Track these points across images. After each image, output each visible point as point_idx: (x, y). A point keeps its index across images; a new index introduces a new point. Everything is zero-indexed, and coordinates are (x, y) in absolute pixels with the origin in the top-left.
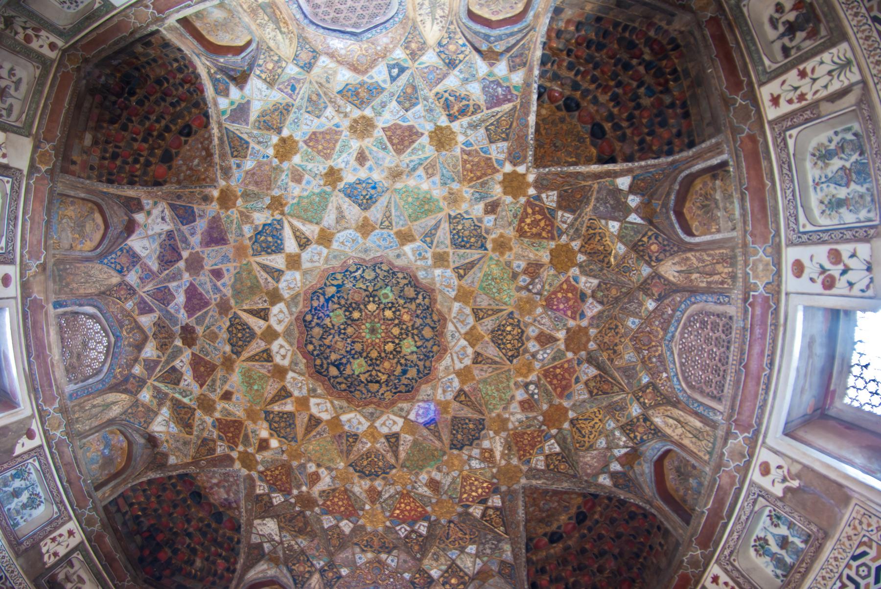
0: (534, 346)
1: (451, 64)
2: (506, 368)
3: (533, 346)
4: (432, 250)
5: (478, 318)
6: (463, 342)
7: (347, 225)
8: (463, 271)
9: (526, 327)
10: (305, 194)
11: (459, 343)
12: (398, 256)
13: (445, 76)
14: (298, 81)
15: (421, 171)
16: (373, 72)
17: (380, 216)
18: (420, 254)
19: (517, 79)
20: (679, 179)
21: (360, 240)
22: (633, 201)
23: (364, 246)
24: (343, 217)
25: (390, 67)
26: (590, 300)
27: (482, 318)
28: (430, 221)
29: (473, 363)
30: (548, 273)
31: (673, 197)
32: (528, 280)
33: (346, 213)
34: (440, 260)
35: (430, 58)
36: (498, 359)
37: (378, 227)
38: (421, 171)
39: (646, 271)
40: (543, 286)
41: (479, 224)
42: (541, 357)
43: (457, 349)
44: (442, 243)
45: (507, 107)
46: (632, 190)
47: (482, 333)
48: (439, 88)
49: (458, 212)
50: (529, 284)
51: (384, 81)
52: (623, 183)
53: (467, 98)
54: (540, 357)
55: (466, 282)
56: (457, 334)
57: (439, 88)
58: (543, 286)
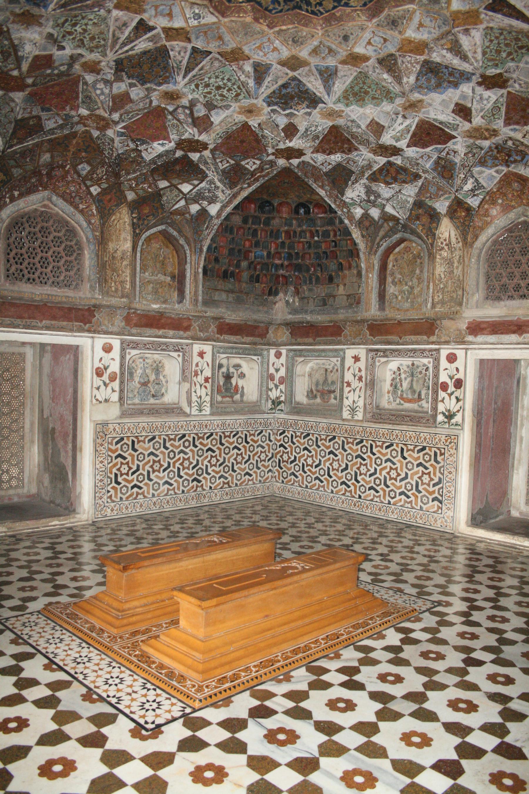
0: (119, 88)
1: (418, 204)
2: (108, 52)
3: (120, 87)
4: (312, 65)
5: (194, 50)
6: (178, 23)
7: (443, 41)
8: (261, 72)
9: (147, 89)
11: (181, 18)
12: (346, 38)
13: (418, 194)
19: (357, 211)
20: (186, 247)
22: (194, 208)
23: (400, 28)
24: (450, 50)
26: (132, 146)
27: (192, 54)
28: (339, 86)
29: (142, 19)
30: (190, 132)
31: (175, 233)
32: (196, 115)
35: (441, 206)
36: (126, 48)
37: (397, 54)
39: (131, 196)
40: (178, 120)
41: (288, 111)
42: (98, 86)
43: (176, 10)
44: (307, 75)
46: (203, 212)
47: (174, 43)
48: (420, 183)
49: (318, 109)
50: (192, 113)
52: (213, 209)
54: (100, 85)
55: (248, 68)
56: (196, 23)
57: (420, 183)
58: (178, 120)
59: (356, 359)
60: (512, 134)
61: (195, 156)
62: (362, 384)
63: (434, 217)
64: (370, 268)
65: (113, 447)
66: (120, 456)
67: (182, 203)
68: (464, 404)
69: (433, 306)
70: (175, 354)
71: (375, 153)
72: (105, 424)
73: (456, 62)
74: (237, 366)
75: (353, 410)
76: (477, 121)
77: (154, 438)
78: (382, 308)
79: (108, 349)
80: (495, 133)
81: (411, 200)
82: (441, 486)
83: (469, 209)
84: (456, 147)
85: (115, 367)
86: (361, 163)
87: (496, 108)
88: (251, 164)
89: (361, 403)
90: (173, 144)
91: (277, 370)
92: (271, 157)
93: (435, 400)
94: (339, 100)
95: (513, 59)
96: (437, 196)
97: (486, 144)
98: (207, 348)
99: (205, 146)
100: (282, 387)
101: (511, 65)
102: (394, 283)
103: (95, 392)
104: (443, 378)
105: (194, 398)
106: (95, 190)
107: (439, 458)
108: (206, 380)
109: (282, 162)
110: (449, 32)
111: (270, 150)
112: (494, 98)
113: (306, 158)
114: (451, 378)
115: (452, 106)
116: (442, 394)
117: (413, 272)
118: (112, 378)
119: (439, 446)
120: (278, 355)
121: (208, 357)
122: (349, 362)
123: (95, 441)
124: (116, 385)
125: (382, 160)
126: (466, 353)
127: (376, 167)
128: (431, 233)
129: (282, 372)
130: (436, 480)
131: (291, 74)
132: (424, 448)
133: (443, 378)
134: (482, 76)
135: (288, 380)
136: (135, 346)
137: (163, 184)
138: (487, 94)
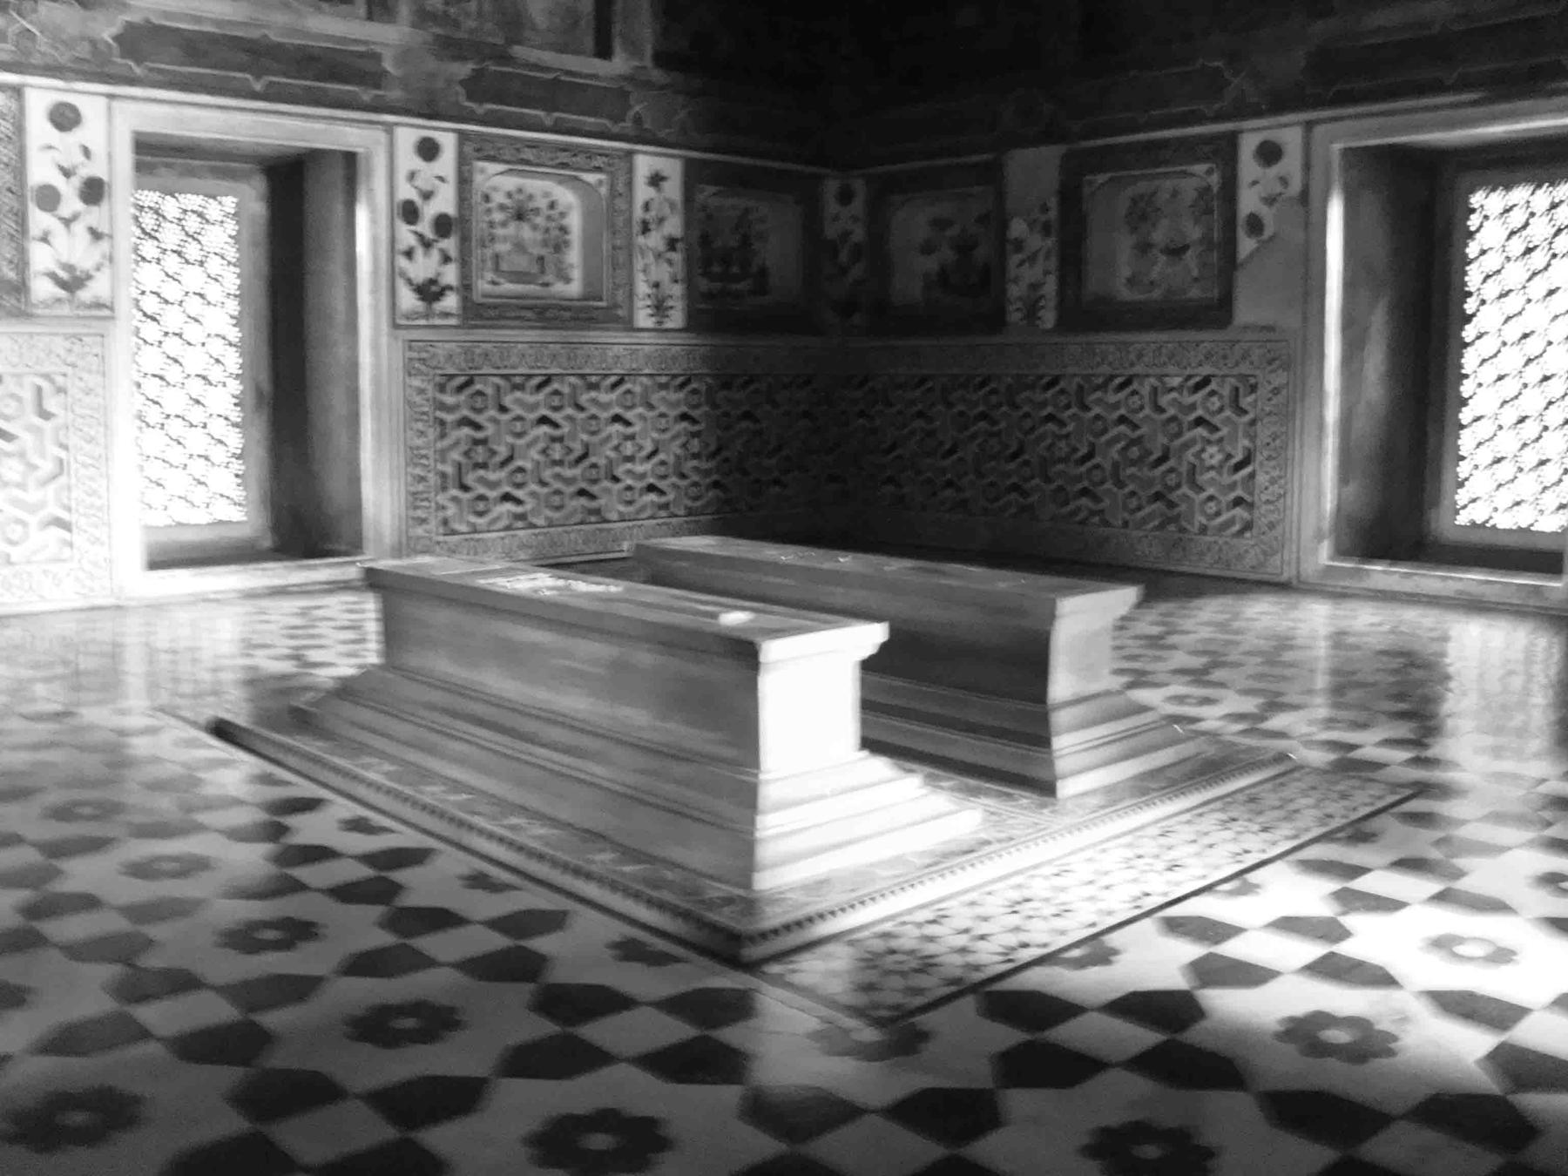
68: (112, 247)
82: (63, 480)
107: (51, 404)
114: (67, 173)
116: (39, 220)
119: (47, 369)
126: (109, 109)
130: (47, 467)
133: (41, 171)
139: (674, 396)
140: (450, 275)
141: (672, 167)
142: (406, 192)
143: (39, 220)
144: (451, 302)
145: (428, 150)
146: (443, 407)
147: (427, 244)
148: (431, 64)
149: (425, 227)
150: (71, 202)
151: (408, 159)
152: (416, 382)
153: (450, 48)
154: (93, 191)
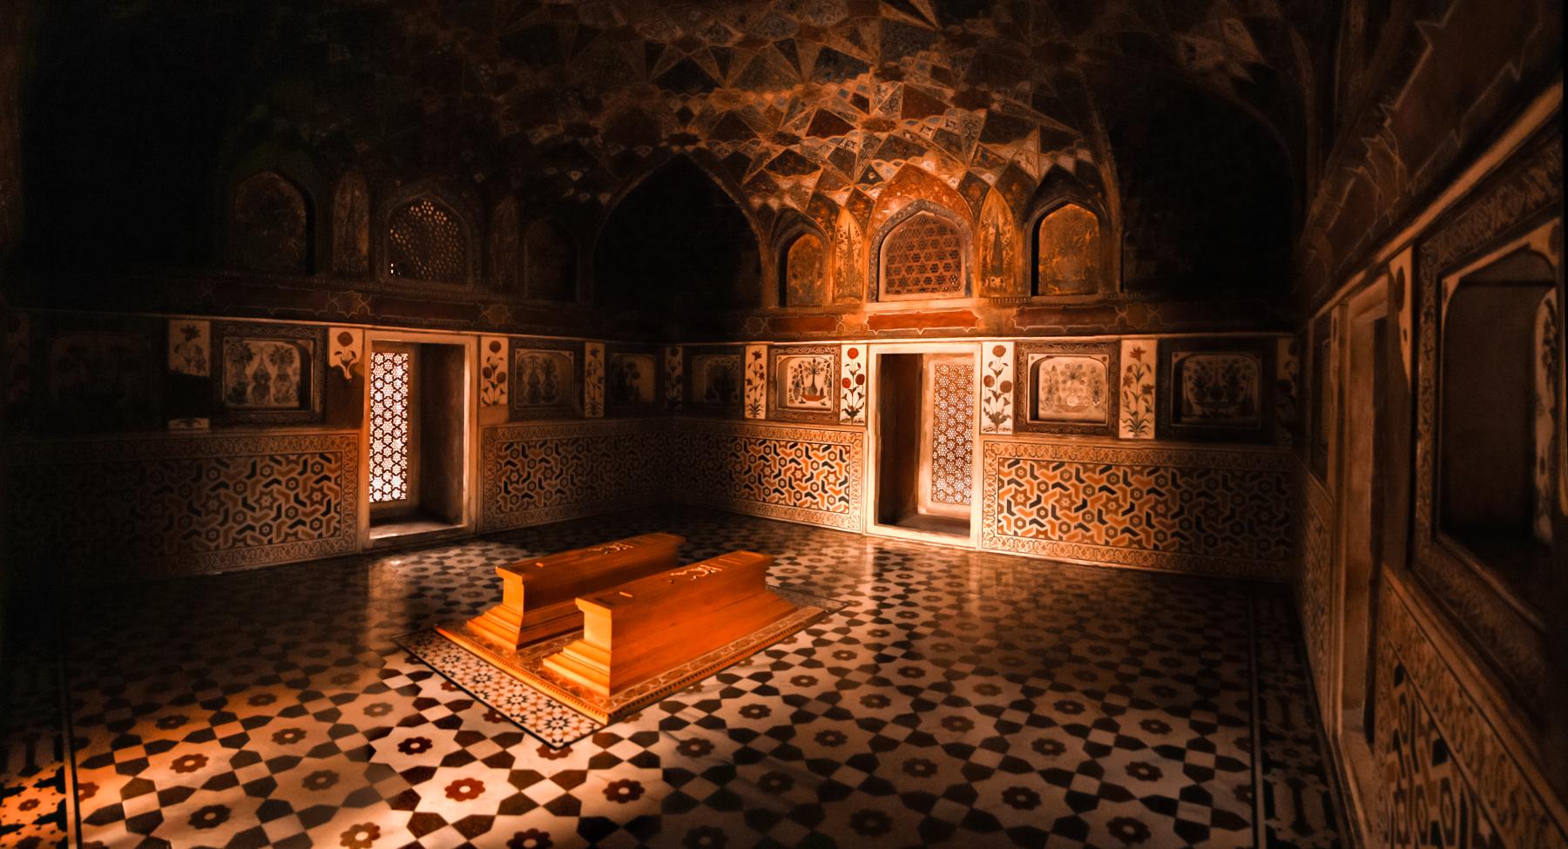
1: (817, 196)
8: (653, 51)
10: (923, 53)
12: (743, 20)
13: (819, 184)
14: (980, 164)
15: (784, 109)
16: (896, 170)
17: (801, 52)
18: (717, 32)
21: (811, 20)
24: (850, 38)
25: (878, 178)
28: (735, 72)
33: (848, 44)
34: (688, 43)
35: (841, 197)
38: (784, 109)
45: (746, 180)
48: (818, 174)
51: (879, 165)
52: (604, 198)
53: (786, 174)
57: (818, 174)
59: (757, 355)
60: (908, 127)
61: (585, 141)
62: (764, 382)
63: (834, 209)
64: (772, 258)
65: (503, 453)
66: (509, 463)
67: (572, 192)
69: (834, 300)
70: (566, 353)
71: (773, 140)
72: (494, 429)
73: (855, 52)
74: (632, 366)
75: (755, 409)
76: (876, 113)
77: (545, 443)
78: (783, 302)
79: (495, 347)
80: (892, 125)
81: (810, 192)
83: (869, 203)
84: (855, 139)
85: (503, 367)
86: (758, 149)
87: (893, 100)
88: (644, 151)
89: (763, 402)
90: (561, 129)
91: (674, 369)
92: (664, 144)
93: (838, 398)
94: (735, 85)
95: (909, 54)
96: (836, 187)
97: (884, 136)
98: (600, 347)
99: (595, 131)
100: (680, 387)
101: (908, 59)
102: (795, 276)
103: (483, 394)
104: (845, 374)
105: (587, 400)
106: (479, 177)
108: (600, 380)
109: (676, 148)
110: (847, 20)
111: (664, 136)
112: (890, 92)
113: (702, 145)
115: (850, 97)
116: (844, 391)
117: (812, 266)
118: (501, 379)
120: (674, 353)
121: (601, 356)
122: (749, 358)
123: (483, 447)
124: (505, 386)
125: (781, 149)
127: (774, 156)
128: (830, 225)
129: (679, 371)
131: (685, 54)
132: (829, 447)
133: (845, 374)
134: (881, 66)
135: (687, 378)
136: (525, 344)
137: (551, 171)
138: (884, 86)
139: (1145, 478)
140: (1009, 410)
141: (1148, 345)
142: (988, 372)
143: (844, 391)
144: (1009, 423)
145: (999, 352)
146: (999, 472)
147: (997, 397)
148: (995, 311)
149: (996, 387)
150: (854, 384)
151: (989, 355)
152: (989, 460)
153: (1002, 304)
154: (860, 379)
